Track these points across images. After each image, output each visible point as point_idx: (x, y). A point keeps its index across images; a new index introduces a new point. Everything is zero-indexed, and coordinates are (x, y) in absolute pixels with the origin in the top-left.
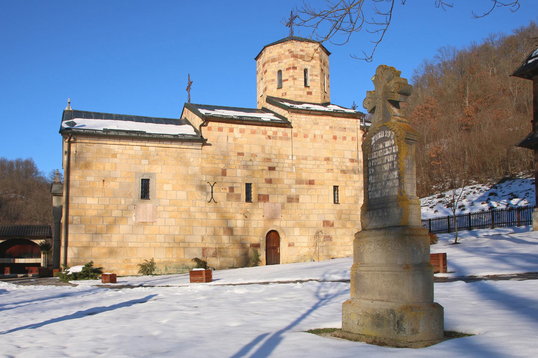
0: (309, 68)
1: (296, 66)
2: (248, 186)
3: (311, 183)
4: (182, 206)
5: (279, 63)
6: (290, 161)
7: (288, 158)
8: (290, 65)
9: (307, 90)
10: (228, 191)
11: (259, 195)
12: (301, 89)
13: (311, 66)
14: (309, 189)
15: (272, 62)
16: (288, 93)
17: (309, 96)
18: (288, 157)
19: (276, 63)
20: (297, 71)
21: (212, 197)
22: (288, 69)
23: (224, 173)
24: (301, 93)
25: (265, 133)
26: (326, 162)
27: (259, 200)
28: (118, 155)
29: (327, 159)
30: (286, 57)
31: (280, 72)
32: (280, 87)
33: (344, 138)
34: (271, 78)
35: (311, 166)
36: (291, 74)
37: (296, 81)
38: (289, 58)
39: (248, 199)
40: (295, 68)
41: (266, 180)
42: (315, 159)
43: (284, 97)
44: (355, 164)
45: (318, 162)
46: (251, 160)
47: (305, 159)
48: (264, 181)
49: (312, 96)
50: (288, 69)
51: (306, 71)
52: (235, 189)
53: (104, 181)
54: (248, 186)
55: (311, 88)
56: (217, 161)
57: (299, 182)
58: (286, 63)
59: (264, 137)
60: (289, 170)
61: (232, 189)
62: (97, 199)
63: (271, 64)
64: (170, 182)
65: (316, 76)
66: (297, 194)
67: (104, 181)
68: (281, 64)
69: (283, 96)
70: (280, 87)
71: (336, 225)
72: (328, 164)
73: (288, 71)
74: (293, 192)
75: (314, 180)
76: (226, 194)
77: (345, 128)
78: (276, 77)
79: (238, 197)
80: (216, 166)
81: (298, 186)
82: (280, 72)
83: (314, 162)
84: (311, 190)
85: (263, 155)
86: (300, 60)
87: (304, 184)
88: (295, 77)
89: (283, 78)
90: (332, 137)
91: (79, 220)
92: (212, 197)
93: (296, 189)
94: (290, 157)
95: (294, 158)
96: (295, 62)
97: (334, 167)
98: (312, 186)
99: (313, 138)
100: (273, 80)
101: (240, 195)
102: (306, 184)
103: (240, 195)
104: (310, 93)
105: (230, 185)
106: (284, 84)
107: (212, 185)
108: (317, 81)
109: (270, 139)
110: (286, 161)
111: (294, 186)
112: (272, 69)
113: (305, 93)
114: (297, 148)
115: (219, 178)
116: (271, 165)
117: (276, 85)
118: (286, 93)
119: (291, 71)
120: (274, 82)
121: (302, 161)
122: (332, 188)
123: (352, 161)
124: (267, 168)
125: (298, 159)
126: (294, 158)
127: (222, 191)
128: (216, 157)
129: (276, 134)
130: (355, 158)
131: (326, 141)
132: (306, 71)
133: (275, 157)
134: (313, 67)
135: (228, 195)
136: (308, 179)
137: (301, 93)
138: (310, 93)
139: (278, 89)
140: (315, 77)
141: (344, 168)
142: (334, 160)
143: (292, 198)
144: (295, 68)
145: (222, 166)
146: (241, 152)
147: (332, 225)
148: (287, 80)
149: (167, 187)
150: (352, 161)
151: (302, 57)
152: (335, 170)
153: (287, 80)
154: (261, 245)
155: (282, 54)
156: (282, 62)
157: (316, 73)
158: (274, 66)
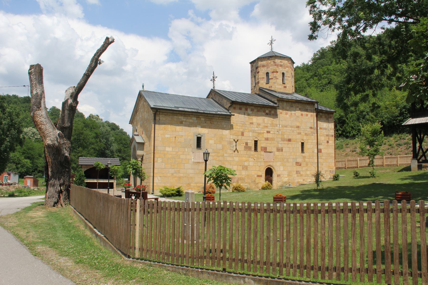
0: (285, 72)
1: (278, 70)
2: (256, 142)
3: (289, 140)
4: (219, 153)
5: (268, 68)
6: (278, 128)
7: (277, 126)
8: (274, 70)
9: (284, 85)
10: (244, 145)
11: (262, 147)
12: (280, 85)
13: (286, 71)
14: (288, 144)
15: (262, 67)
16: (273, 86)
17: (285, 88)
18: (277, 125)
19: (265, 68)
20: (278, 74)
21: (236, 149)
22: (273, 72)
23: (243, 134)
24: (280, 87)
25: (264, 112)
26: (297, 129)
27: (262, 150)
28: (183, 122)
29: (298, 127)
30: (272, 65)
31: (267, 73)
32: (268, 83)
33: (307, 115)
34: (262, 77)
35: (289, 131)
36: (275, 76)
37: (278, 80)
38: (273, 66)
39: (256, 149)
40: (277, 72)
41: (265, 138)
42: (292, 127)
43: (270, 89)
44: (312, 130)
45: (293, 129)
46: (257, 127)
47: (286, 127)
48: (264, 139)
49: (286, 89)
50: (273, 72)
51: (283, 74)
52: (249, 144)
53: (175, 137)
54: (256, 142)
55: (286, 84)
56: (239, 127)
57: (283, 140)
58: (271, 69)
59: (264, 114)
60: (277, 133)
61: (247, 144)
62: (172, 148)
63: (262, 68)
64: (213, 139)
65: (289, 77)
66: (282, 146)
67: (175, 137)
68: (268, 69)
69: (269, 88)
70: (268, 83)
71: (302, 165)
72: (298, 130)
73: (273, 74)
74: (280, 146)
75: (291, 139)
76: (243, 147)
77: (307, 109)
78: (265, 76)
79: (250, 148)
80: (238, 130)
81: (282, 142)
82: (267, 73)
83: (291, 129)
84: (289, 145)
86: (280, 67)
87: (285, 141)
88: (277, 77)
89: (270, 77)
90: (300, 114)
91: (161, 160)
92: (236, 149)
93: (281, 144)
94: (278, 126)
95: (280, 126)
96: (277, 68)
97: (302, 132)
98: (290, 143)
99: (290, 115)
100: (263, 78)
101: (251, 147)
102: (287, 141)
103: (251, 147)
104: (285, 87)
105: (246, 141)
106: (270, 81)
107: (236, 141)
108: (289, 80)
109: (267, 115)
110: (276, 128)
111: (280, 142)
112: (263, 71)
113: (283, 87)
114: (282, 121)
115: (240, 137)
116: (268, 130)
117: (265, 81)
118: (271, 87)
119: (275, 74)
120: (264, 79)
121: (285, 128)
122: (300, 143)
123: (311, 128)
124: (266, 132)
125: (282, 127)
126: (280, 126)
127: (242, 144)
128: (238, 125)
129: (271, 112)
130: (313, 126)
131: (298, 117)
132: (283, 74)
133: (270, 125)
134: (287, 72)
135: (245, 147)
136: (288, 138)
137: (280, 87)
138: (285, 87)
139: (266, 84)
140: (288, 78)
141: (307, 132)
142: (301, 127)
143: (279, 149)
144: (277, 72)
145: (241, 130)
146: (251, 122)
147: (300, 165)
148: (272, 79)
149: (211, 142)
150: (311, 128)
151: (281, 66)
152: (302, 134)
153: (272, 79)
154: (263, 176)
155: (269, 63)
156: (269, 68)
157: (288, 75)
158: (264, 70)
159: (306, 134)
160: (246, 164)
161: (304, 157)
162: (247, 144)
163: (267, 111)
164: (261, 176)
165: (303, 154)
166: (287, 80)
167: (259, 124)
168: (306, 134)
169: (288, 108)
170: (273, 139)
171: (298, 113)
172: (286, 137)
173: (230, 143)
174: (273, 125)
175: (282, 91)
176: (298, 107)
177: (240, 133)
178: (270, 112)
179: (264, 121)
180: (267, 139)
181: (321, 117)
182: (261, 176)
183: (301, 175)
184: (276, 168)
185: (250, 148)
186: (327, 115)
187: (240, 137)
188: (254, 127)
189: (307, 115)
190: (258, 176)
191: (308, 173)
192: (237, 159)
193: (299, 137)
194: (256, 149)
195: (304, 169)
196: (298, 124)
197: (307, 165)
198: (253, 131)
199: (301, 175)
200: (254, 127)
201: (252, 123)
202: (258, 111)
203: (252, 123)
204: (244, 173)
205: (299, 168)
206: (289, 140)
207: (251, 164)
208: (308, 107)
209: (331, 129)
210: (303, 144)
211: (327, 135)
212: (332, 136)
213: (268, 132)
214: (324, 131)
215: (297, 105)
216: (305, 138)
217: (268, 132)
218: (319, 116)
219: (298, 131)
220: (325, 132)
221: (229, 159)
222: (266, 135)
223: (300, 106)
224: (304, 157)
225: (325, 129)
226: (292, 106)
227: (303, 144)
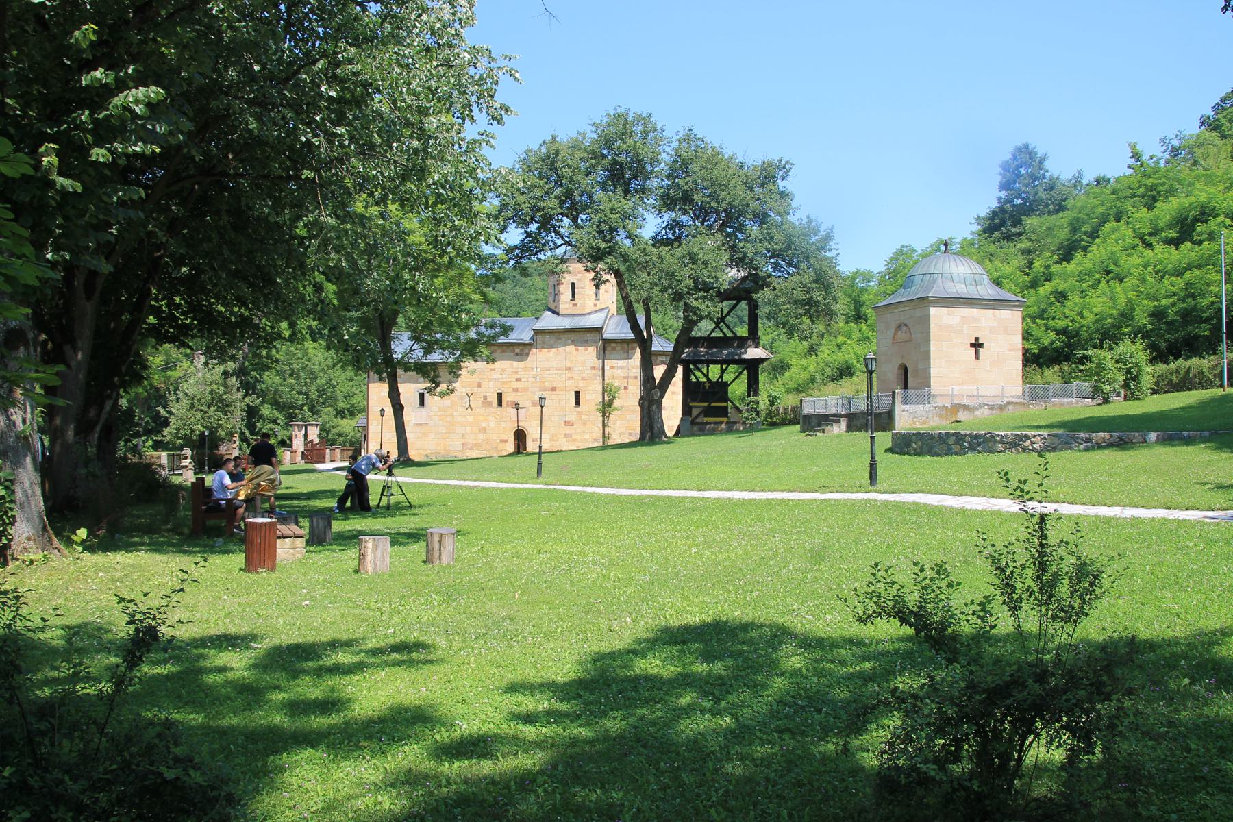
2: (500, 395)
3: (554, 389)
23: (479, 385)
29: (569, 369)
39: (500, 404)
44: (593, 371)
51: (573, 285)
54: (500, 395)
57: (544, 389)
61: (485, 398)
85: (511, 370)
104: (575, 305)
115: (475, 390)
123: (594, 368)
132: (573, 285)
134: (579, 280)
138: (575, 305)
150: (594, 368)
159: (583, 379)
160: (484, 425)
161: (580, 414)
162: (485, 398)
163: (517, 351)
164: (506, 441)
165: (578, 409)
166: (579, 293)
167: (503, 370)
168: (583, 379)
169: (552, 342)
170: (525, 389)
171: (570, 348)
172: (547, 384)
173: (462, 398)
174: (525, 369)
175: (568, 312)
176: (567, 340)
177: (476, 385)
178: (522, 350)
179: (512, 365)
180: (516, 390)
181: (614, 349)
182: (506, 441)
183: (574, 440)
184: (529, 429)
185: (490, 404)
186: (626, 345)
187: (475, 390)
188: (496, 375)
189: (586, 350)
190: (502, 441)
191: (587, 436)
192: (470, 419)
193: (569, 383)
194: (500, 404)
195: (579, 430)
196: (568, 365)
197: (585, 424)
198: (496, 380)
199: (574, 440)
200: (496, 375)
201: (494, 370)
202: (503, 352)
203: (494, 370)
204: (481, 437)
205: (569, 430)
206: (554, 389)
207: (492, 424)
208: (589, 336)
209: (633, 367)
210: (577, 394)
211: (624, 378)
212: (636, 378)
213: (518, 380)
214: (619, 371)
215: (567, 335)
216: (581, 384)
217: (518, 380)
218: (609, 349)
219: (568, 375)
220: (620, 373)
221: (459, 419)
222: (515, 385)
223: (573, 336)
224: (580, 414)
225: (622, 368)
226: (560, 339)
227: (577, 394)
